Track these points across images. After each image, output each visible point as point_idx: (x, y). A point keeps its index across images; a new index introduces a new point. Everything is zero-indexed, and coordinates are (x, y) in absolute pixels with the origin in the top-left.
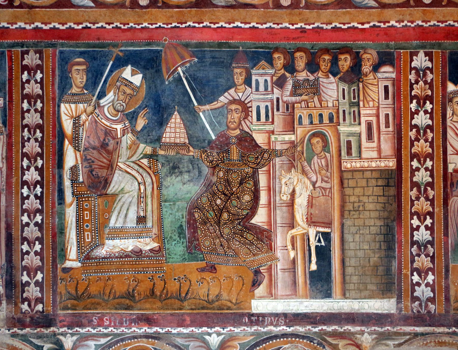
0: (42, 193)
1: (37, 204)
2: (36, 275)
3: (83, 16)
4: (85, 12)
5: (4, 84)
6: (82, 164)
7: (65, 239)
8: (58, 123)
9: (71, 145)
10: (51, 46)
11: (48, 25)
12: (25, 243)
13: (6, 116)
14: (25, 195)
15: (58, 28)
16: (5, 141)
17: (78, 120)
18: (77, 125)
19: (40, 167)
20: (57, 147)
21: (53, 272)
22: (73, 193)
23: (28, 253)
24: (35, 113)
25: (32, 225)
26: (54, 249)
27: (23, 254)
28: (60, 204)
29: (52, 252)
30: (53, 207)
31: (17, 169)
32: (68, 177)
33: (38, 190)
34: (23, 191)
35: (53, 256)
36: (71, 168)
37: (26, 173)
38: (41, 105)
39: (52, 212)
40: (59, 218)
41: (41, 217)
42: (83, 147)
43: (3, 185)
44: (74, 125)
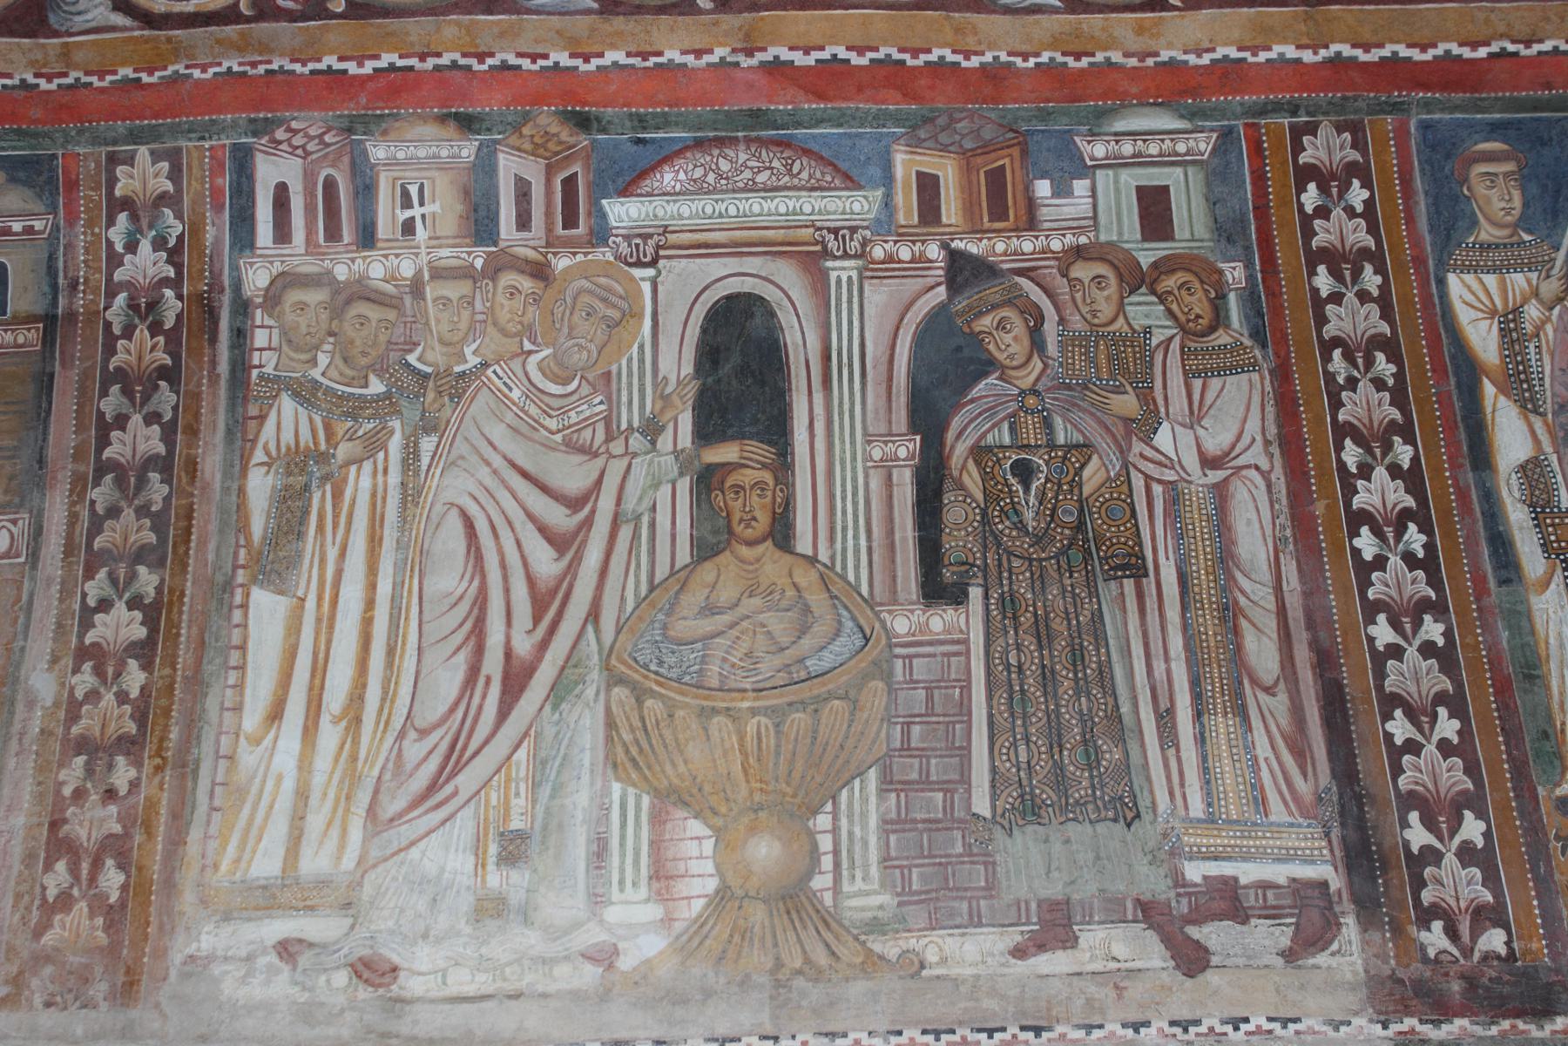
0: (1429, 547)
1: (1418, 586)
2: (1460, 825)
3: (1487, 21)
4: (1492, 10)
5: (1243, 221)
6: (1557, 452)
7: (1549, 696)
8: (1446, 332)
9: (1507, 396)
10: (1387, 108)
11: (1373, 50)
12: (1398, 713)
13: (1260, 315)
14: (1368, 555)
15: (1409, 59)
16: (1268, 388)
17: (1514, 320)
18: (1514, 335)
19: (1406, 467)
20: (1457, 405)
21: (1522, 816)
22: (1545, 546)
23: (1412, 747)
24: (1362, 305)
25: (1411, 653)
26: (1513, 735)
27: (1397, 752)
28: (1503, 582)
29: (1507, 744)
30: (1481, 590)
31: (1323, 473)
32: (1517, 494)
33: (1415, 538)
34: (1357, 542)
35: (1511, 759)
36: (1523, 468)
37: (1359, 487)
38: (1378, 280)
39: (1479, 609)
40: (1510, 628)
41: (1441, 628)
42: (1549, 401)
43: (1283, 527)
44: (1504, 336)
